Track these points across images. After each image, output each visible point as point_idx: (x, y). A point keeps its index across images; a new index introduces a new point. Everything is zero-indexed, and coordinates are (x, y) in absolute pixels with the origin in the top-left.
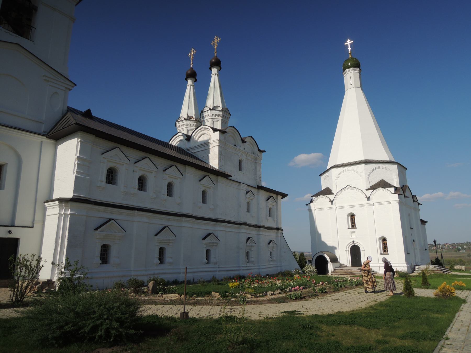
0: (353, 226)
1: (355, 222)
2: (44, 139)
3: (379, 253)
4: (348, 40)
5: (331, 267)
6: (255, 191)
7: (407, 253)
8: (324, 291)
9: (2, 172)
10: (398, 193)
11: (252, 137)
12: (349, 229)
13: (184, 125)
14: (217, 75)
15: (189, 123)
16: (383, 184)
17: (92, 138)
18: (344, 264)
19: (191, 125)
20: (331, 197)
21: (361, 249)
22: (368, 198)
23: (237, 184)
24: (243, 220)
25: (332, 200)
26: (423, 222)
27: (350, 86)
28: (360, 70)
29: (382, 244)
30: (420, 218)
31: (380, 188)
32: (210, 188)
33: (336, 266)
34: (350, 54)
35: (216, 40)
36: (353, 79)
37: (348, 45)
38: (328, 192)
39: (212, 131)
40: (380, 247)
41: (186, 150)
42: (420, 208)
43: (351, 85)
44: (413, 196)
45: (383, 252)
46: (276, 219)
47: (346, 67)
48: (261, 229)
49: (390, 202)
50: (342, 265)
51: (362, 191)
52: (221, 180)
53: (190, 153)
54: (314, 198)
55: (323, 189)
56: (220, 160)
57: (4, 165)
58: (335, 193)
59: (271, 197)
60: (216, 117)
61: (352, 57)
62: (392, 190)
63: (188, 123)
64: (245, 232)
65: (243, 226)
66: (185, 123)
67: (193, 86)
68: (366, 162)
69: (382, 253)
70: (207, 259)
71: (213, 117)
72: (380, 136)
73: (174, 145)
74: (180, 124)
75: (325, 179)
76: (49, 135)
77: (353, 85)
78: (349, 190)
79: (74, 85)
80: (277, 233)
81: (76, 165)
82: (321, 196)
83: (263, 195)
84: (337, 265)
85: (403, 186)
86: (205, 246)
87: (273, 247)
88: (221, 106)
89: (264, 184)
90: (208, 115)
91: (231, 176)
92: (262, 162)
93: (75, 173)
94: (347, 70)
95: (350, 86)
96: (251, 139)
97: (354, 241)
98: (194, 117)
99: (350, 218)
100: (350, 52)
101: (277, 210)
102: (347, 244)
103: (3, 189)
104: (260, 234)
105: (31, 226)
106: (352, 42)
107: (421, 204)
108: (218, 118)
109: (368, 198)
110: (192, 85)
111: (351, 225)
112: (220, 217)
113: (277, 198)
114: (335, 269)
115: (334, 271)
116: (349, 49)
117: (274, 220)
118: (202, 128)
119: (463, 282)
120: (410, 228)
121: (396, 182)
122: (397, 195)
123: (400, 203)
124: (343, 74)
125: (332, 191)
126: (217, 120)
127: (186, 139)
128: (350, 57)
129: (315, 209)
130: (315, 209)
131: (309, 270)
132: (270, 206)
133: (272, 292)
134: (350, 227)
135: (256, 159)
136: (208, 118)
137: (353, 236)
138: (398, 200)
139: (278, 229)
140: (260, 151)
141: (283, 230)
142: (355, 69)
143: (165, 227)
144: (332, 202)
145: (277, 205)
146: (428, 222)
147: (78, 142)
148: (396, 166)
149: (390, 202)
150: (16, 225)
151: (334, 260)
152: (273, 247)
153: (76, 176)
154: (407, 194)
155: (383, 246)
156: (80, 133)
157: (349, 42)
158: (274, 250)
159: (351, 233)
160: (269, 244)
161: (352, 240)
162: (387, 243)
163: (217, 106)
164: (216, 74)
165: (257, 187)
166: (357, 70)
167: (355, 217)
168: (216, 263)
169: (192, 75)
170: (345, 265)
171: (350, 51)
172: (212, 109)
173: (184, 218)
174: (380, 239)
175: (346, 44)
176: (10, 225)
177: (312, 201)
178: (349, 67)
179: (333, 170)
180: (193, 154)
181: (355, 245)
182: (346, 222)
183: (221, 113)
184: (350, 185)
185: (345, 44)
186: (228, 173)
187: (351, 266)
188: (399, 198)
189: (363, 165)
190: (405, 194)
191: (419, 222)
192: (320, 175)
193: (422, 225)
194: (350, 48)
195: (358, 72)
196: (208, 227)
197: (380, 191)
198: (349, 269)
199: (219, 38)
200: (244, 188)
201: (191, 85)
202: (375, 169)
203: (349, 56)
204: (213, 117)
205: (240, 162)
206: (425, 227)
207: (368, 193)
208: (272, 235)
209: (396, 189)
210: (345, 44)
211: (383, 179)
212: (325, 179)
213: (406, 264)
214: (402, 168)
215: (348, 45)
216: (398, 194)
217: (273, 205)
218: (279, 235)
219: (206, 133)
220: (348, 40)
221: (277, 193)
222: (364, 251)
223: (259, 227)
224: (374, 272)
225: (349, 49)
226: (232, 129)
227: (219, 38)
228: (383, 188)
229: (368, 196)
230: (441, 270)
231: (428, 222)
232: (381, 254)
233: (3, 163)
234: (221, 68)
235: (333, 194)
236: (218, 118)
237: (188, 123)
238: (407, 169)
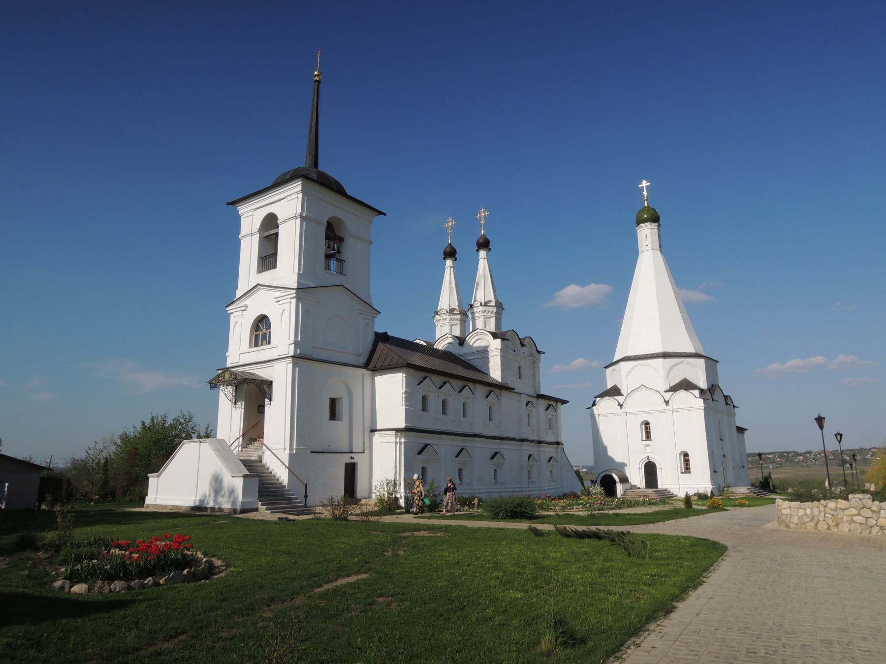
0: (648, 437)
1: (650, 432)
2: (364, 371)
3: (679, 471)
4: (644, 181)
5: (620, 489)
6: (534, 400)
7: (714, 471)
8: (619, 507)
9: (336, 404)
10: (704, 397)
11: (530, 337)
12: (642, 440)
13: (446, 319)
14: (486, 260)
15: (452, 316)
16: (686, 385)
17: (412, 371)
18: (636, 486)
19: (454, 319)
20: (620, 399)
21: (658, 466)
22: (667, 403)
23: (517, 395)
24: (524, 436)
25: (621, 404)
26: (741, 430)
27: (646, 248)
28: (659, 226)
29: (684, 460)
30: (735, 424)
31: (682, 390)
32: (494, 404)
33: (627, 488)
34: (646, 201)
35: (483, 214)
36: (649, 238)
37: (643, 187)
38: (615, 392)
39: (492, 338)
40: (681, 464)
41: (458, 356)
43: (647, 246)
44: (726, 397)
45: (685, 470)
46: (556, 432)
47: (640, 221)
48: (542, 444)
49: (694, 408)
50: (634, 486)
51: (659, 392)
52: (505, 393)
53: (464, 359)
54: (598, 399)
55: (609, 387)
56: (502, 372)
57: (339, 398)
58: (625, 395)
59: (550, 405)
60: (489, 314)
61: (648, 206)
62: (696, 392)
63: (451, 317)
64: (527, 448)
65: (525, 443)
66: (448, 317)
67: (453, 267)
68: (666, 355)
69: (683, 471)
70: (495, 479)
71: (485, 314)
72: (684, 319)
73: (440, 348)
74: (441, 318)
75: (611, 374)
76: (366, 366)
77: (650, 247)
78: (644, 391)
79: (377, 313)
80: (557, 448)
81: (404, 398)
82: (607, 398)
83: (543, 403)
84: (627, 486)
85: (713, 385)
86: (493, 466)
87: (553, 465)
88: (493, 300)
89: (543, 392)
90: (479, 311)
91: (514, 389)
92: (540, 365)
93: (404, 405)
94: (641, 225)
95: (646, 248)
96: (530, 340)
97: (648, 457)
98: (457, 308)
99: (643, 426)
100: (645, 199)
101: (557, 420)
102: (641, 459)
103: (342, 420)
104: (541, 451)
105: (362, 451)
106: (649, 184)
107: (738, 407)
108: (491, 315)
109: (667, 403)
110: (452, 267)
111: (646, 435)
112: (505, 435)
113: (557, 405)
114: (625, 492)
115: (624, 494)
116: (645, 193)
117: (554, 433)
118: (478, 332)
119: (746, 500)
120: (721, 440)
121: (703, 384)
122: (702, 400)
123: (705, 410)
124: (637, 228)
125: (621, 392)
126: (490, 318)
127: (459, 344)
128: (646, 205)
129: (599, 415)
130: (599, 415)
131: (596, 492)
132: (549, 416)
133: (577, 507)
134: (644, 439)
135: (534, 362)
136: (479, 315)
137: (648, 449)
138: (703, 405)
139: (558, 443)
140: (539, 352)
141: (563, 445)
142: (653, 224)
143: (462, 449)
144: (621, 406)
145: (557, 415)
146: (747, 430)
147: (403, 377)
148: (702, 361)
149: (694, 408)
150: (354, 452)
151: (624, 480)
152: (553, 465)
153: (405, 409)
154: (717, 396)
155: (684, 463)
156: (404, 370)
157: (644, 184)
158: (554, 468)
159: (646, 446)
160: (549, 461)
161: (646, 456)
162: (689, 459)
163: (490, 301)
164: (484, 259)
165: (536, 396)
166: (655, 226)
167: (651, 425)
168: (502, 484)
169: (451, 253)
170: (638, 486)
171: (646, 196)
172: (483, 304)
173: (477, 439)
174: (681, 454)
175: (641, 187)
176: (348, 451)
177: (594, 404)
178: (644, 221)
179: (622, 363)
180: (468, 361)
181: (650, 462)
182: (638, 431)
183: (494, 309)
184: (645, 385)
185: (640, 186)
186: (510, 385)
187: (645, 487)
188: (705, 403)
189: (661, 359)
190: (713, 397)
192: (605, 368)
193: (740, 435)
194: (647, 192)
195: (657, 228)
196: (494, 446)
197: (682, 394)
198: (642, 492)
199: (486, 211)
200: (525, 399)
201: (451, 267)
202: (676, 365)
203: (645, 204)
204: (485, 314)
205: (519, 368)
207: (667, 396)
208: (550, 451)
209: (702, 391)
210: (640, 186)
211: (687, 378)
212: (611, 374)
213: (712, 485)
214: (711, 363)
215: (643, 187)
216: (704, 399)
217: (553, 415)
218: (560, 450)
219: (483, 338)
220: (644, 181)
221: (557, 400)
222: (661, 468)
223: (540, 442)
224: (673, 494)
225: (645, 193)
226: (512, 333)
227: (486, 211)
228: (685, 390)
229: (667, 400)
230: (754, 493)
231: (747, 430)
232: (682, 473)
233: (338, 397)
234: (490, 250)
235: (622, 395)
236: (491, 315)
237: (451, 317)
238: (718, 362)
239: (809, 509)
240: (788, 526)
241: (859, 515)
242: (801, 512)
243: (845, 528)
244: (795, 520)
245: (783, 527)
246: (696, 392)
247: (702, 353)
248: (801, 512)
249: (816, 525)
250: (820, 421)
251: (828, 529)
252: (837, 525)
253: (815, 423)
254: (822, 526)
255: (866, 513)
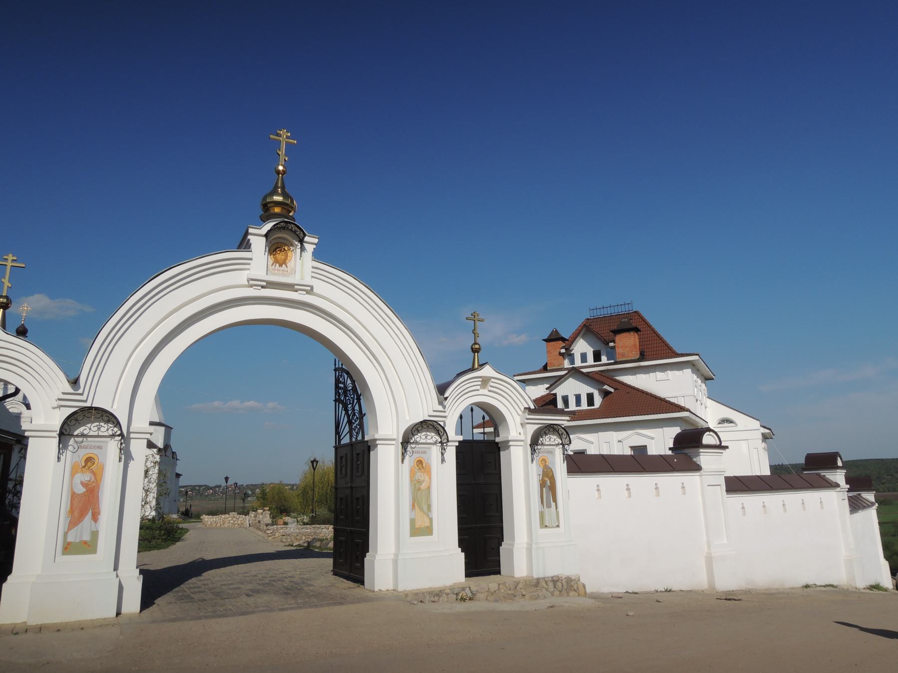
26: (178, 475)
39: (26, 409)
42: (177, 463)
44: (174, 453)
85: (166, 445)
121: (160, 445)
146: (182, 475)
148: (163, 429)
154: (169, 453)
191: (175, 475)
206: (179, 480)
209: (160, 450)
214: (168, 429)
216: (160, 456)
231: (182, 475)
238: (172, 428)
239: (215, 518)
240: (206, 526)
241: (232, 520)
242: (212, 520)
243: (226, 525)
244: (209, 523)
245: (204, 526)
246: (155, 450)
247: (163, 422)
248: (212, 520)
249: (217, 524)
250: (227, 479)
251: (220, 526)
252: (224, 524)
253: (224, 479)
254: (218, 525)
255: (235, 519)
